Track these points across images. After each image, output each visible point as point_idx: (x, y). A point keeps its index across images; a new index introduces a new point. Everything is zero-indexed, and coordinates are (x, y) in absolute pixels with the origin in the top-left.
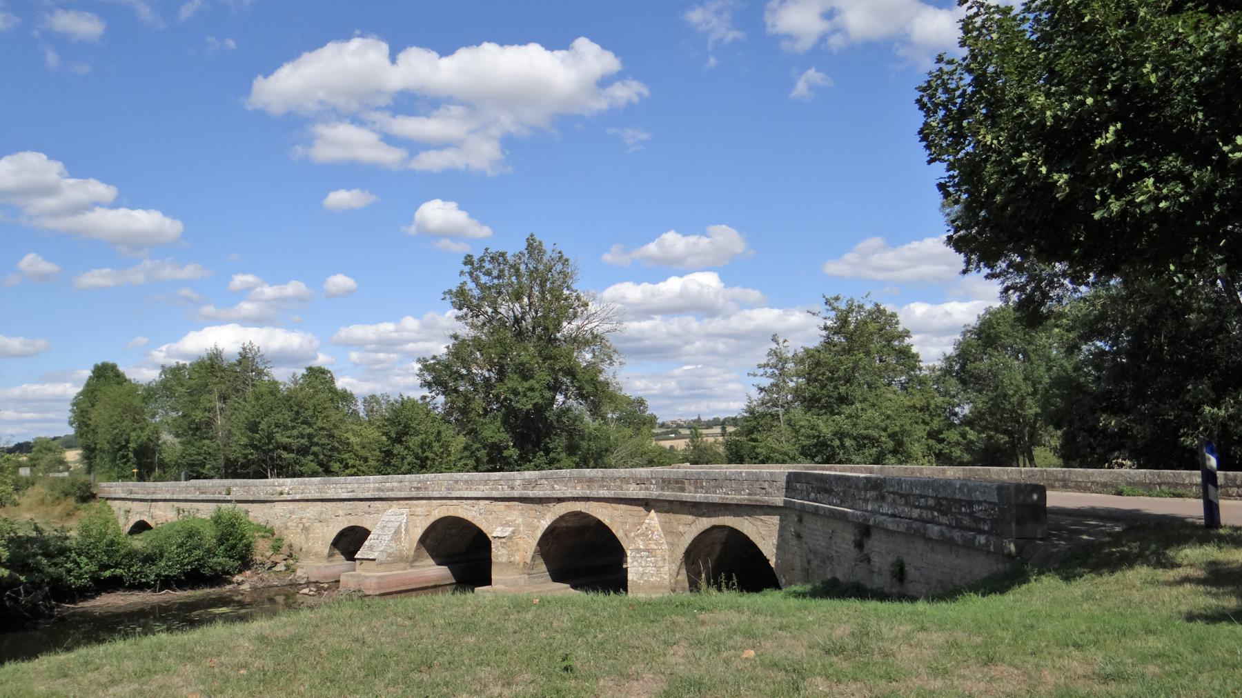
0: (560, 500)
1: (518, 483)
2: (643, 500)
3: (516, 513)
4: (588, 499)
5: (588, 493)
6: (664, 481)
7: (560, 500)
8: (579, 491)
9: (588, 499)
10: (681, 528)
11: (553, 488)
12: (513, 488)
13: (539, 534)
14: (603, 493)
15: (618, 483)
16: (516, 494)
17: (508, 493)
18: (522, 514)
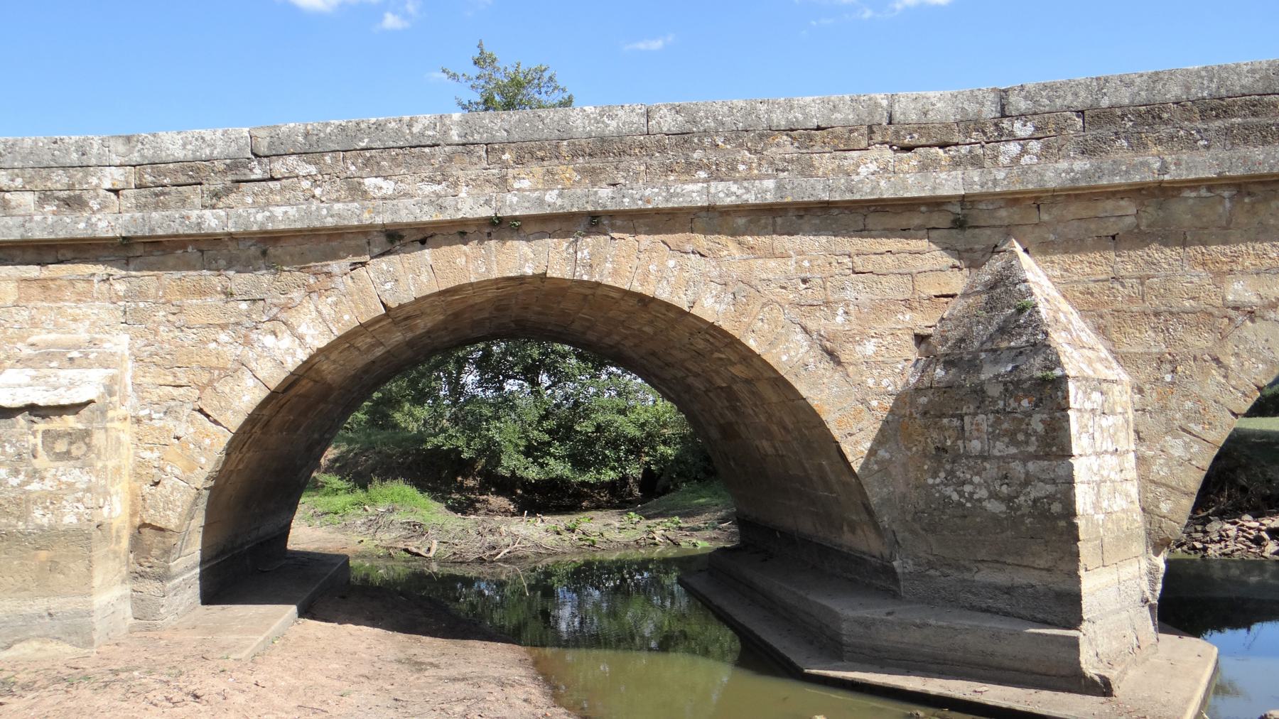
0: (396, 238)
1: (112, 177)
2: (936, 203)
3: (99, 311)
4: (595, 222)
5: (605, 197)
6: (1095, 117)
7: (396, 238)
8: (526, 192)
9: (597, 222)
10: (1240, 290)
11: (356, 191)
12: (74, 202)
13: (245, 396)
14: (693, 192)
15: (785, 148)
16: (105, 223)
17: (44, 223)
18: (130, 319)
